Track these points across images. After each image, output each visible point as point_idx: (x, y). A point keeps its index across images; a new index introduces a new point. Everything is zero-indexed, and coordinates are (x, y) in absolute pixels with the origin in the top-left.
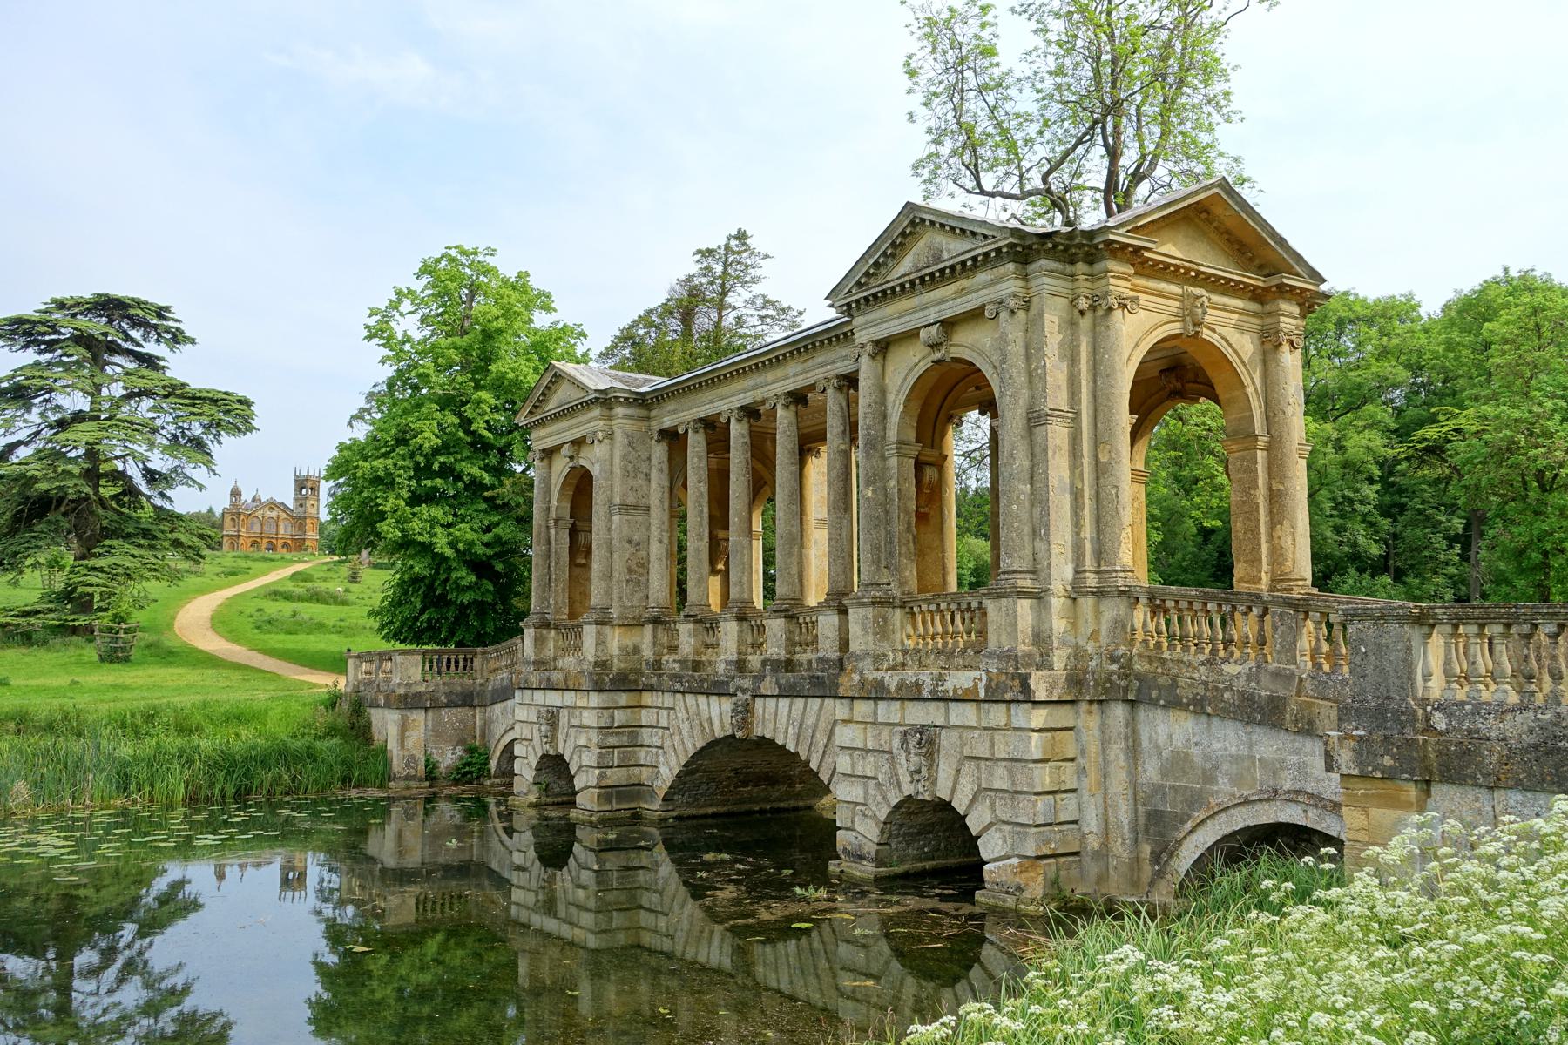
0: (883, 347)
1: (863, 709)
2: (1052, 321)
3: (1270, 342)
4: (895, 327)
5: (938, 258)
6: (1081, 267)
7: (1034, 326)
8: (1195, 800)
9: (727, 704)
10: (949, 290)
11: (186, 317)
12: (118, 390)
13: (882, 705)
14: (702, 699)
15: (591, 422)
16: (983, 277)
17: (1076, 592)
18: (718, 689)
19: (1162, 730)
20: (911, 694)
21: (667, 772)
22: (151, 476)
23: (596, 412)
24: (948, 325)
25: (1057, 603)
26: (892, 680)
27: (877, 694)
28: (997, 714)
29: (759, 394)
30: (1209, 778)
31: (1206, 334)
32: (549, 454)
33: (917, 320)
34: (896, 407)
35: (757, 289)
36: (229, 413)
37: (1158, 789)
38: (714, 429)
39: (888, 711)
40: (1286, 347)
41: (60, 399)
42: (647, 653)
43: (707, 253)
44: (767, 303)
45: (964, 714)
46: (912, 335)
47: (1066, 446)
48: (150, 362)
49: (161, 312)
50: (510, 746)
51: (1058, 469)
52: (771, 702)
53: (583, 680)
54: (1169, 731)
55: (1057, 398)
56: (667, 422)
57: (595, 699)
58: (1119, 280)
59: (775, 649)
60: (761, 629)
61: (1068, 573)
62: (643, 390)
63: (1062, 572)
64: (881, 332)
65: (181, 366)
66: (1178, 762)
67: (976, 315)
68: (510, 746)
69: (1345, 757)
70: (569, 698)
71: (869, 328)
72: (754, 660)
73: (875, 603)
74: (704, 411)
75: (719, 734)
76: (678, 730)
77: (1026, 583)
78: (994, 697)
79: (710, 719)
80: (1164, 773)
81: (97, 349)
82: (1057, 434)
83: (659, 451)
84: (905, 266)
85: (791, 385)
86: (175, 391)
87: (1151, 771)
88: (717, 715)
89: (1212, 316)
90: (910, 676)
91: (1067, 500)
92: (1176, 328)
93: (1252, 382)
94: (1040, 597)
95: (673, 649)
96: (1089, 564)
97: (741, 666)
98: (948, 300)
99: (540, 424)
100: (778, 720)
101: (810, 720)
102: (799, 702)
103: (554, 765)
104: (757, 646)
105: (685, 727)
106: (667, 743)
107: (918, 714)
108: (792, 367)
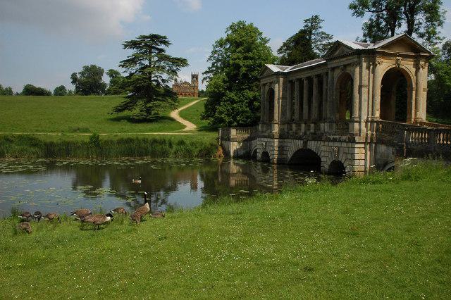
0: (333, 69)
1: (326, 143)
2: (364, 65)
3: (417, 67)
4: (335, 65)
6: (371, 55)
7: (361, 68)
10: (344, 59)
11: (169, 39)
12: (156, 59)
15: (274, 78)
17: (367, 122)
18: (300, 138)
20: (335, 140)
21: (290, 156)
22: (163, 81)
24: (345, 66)
25: (363, 124)
26: (332, 137)
27: (329, 140)
28: (350, 145)
29: (310, 75)
31: (401, 66)
32: (264, 85)
33: (339, 64)
34: (336, 80)
35: (320, 30)
36: (182, 62)
38: (300, 81)
39: (331, 144)
40: (421, 69)
41: (143, 62)
42: (286, 130)
43: (306, 21)
44: (323, 33)
45: (344, 145)
46: (339, 67)
47: (367, 91)
48: (162, 50)
49: (165, 37)
50: (256, 150)
51: (365, 97)
55: (365, 82)
56: (291, 79)
58: (378, 59)
59: (312, 131)
60: (310, 126)
61: (366, 118)
62: (285, 71)
63: (364, 117)
64: (333, 66)
65: (170, 51)
67: (349, 65)
68: (256, 150)
69: (395, 152)
70: (269, 140)
72: (308, 132)
73: (329, 122)
74: (298, 77)
76: (294, 146)
77: (358, 119)
78: (349, 141)
81: (150, 48)
82: (365, 90)
83: (289, 85)
85: (316, 73)
86: (168, 58)
87: (378, 156)
88: (300, 143)
89: (402, 63)
91: (366, 103)
92: (394, 66)
93: (413, 78)
94: (360, 122)
95: (291, 130)
96: (370, 115)
97: (305, 134)
98: (344, 61)
99: (262, 78)
100: (312, 145)
103: (265, 154)
104: (309, 130)
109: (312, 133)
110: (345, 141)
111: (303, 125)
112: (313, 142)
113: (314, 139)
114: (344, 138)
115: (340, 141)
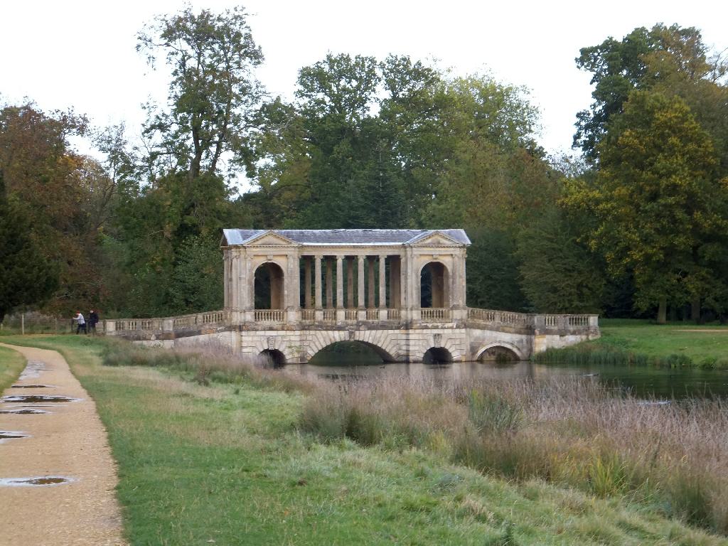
1: (418, 331)
5: (439, 243)
8: (480, 344)
9: (342, 333)
13: (425, 330)
14: (330, 332)
16: (452, 249)
18: (340, 329)
19: (474, 333)
20: (437, 328)
23: (293, 249)
26: (430, 325)
27: (426, 328)
28: (457, 331)
30: (484, 340)
37: (472, 343)
45: (450, 331)
52: (362, 332)
53: (293, 327)
54: (477, 332)
57: (298, 333)
66: (477, 338)
71: (416, 252)
75: (338, 340)
78: (458, 327)
79: (334, 337)
80: (475, 340)
84: (429, 241)
88: (338, 336)
90: (435, 324)
100: (366, 336)
101: (378, 336)
102: (374, 332)
105: (322, 340)
106: (312, 344)
107: (436, 331)
108: (368, 250)
109: (364, 323)
110: (452, 328)
111: (341, 314)
112: (368, 332)
113: (369, 329)
114: (450, 325)
115: (445, 328)
